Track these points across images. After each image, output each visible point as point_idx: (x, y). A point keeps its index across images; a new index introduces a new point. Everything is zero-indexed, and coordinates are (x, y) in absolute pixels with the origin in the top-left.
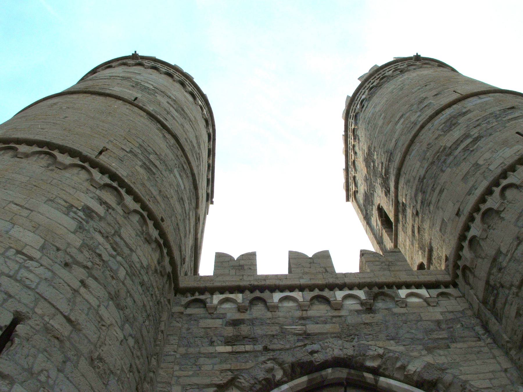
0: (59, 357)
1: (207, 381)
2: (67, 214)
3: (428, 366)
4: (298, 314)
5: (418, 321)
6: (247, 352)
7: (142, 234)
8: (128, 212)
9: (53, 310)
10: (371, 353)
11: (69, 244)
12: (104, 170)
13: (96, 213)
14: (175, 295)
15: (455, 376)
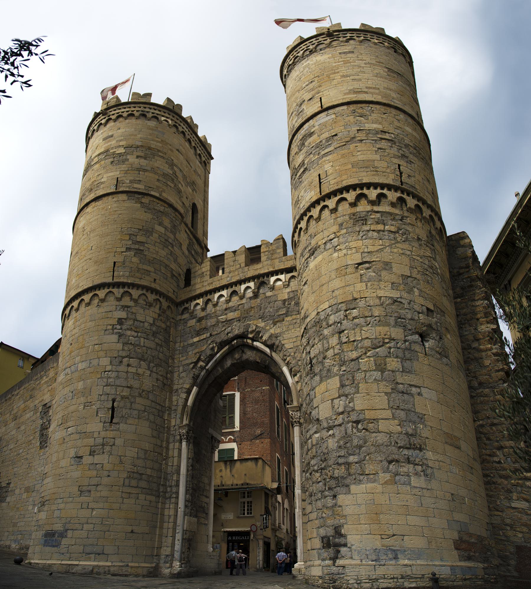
0: (129, 405)
1: (190, 361)
2: (113, 333)
3: (271, 336)
4: (225, 306)
5: (275, 301)
6: (204, 339)
7: (146, 305)
8: (136, 301)
9: (122, 388)
10: (250, 330)
11: (118, 351)
12: (118, 285)
13: (124, 319)
14: (177, 307)
15: (280, 341)
